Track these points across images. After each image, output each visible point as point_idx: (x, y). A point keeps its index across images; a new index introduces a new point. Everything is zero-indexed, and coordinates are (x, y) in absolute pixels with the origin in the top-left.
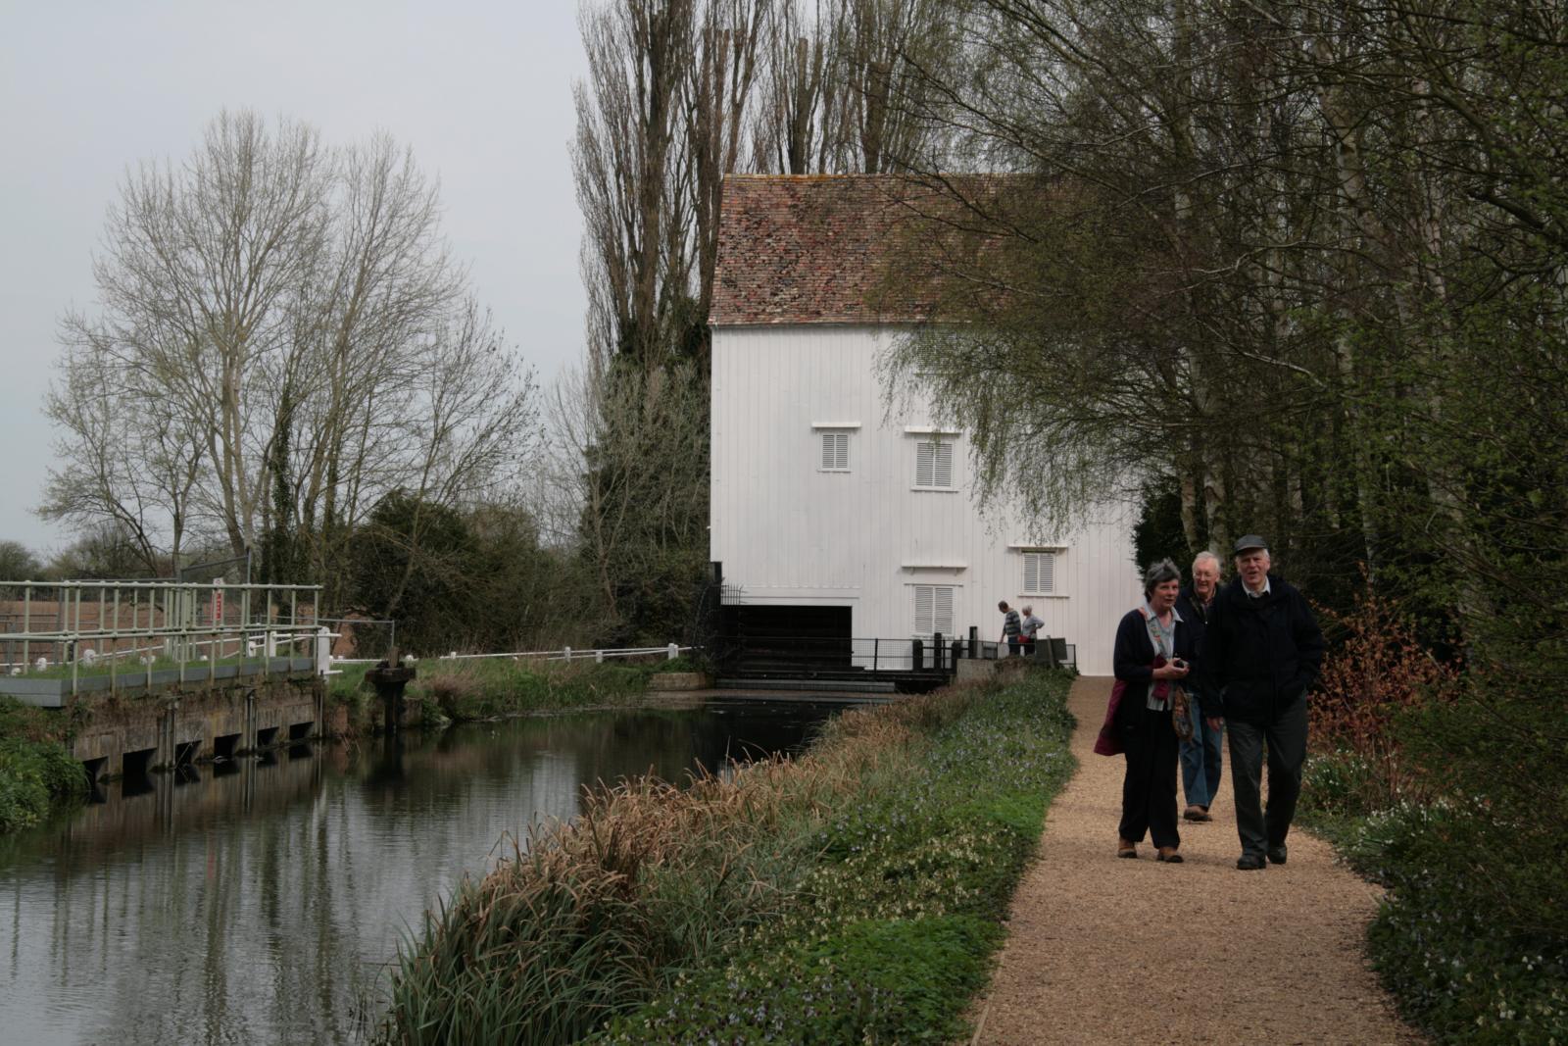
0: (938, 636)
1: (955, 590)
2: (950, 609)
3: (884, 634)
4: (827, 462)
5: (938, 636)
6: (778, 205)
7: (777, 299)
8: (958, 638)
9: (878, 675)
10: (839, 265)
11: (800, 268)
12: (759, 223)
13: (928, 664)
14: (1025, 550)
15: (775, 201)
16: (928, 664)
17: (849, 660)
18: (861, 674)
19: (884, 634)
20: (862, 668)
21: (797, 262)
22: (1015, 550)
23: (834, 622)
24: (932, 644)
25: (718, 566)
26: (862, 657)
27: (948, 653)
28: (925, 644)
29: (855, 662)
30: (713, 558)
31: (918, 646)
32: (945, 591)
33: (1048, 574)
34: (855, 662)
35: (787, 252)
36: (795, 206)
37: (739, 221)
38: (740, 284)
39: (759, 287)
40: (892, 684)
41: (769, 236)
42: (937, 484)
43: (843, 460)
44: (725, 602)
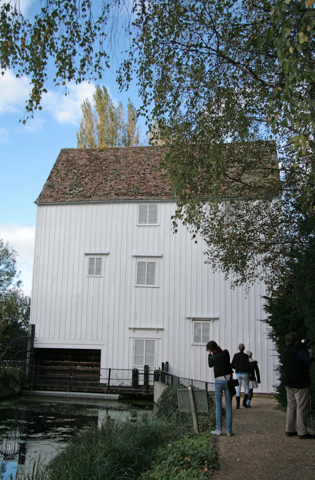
0: (146, 367)
1: (156, 341)
2: (153, 352)
3: (118, 365)
4: (91, 271)
5: (146, 367)
6: (82, 159)
7: (72, 192)
8: (157, 369)
9: (111, 389)
10: (105, 179)
11: (86, 180)
12: (72, 165)
13: (141, 383)
14: (194, 319)
15: (81, 157)
16: (141, 383)
17: (99, 380)
19: (118, 365)
21: (85, 178)
22: (189, 318)
24: (143, 372)
25: (33, 326)
27: (151, 378)
28: (140, 372)
29: (101, 381)
30: (31, 322)
31: (135, 373)
32: (150, 342)
33: (207, 331)
34: (101, 381)
35: (81, 174)
36: (90, 158)
37: (63, 164)
38: (56, 187)
39: (65, 188)
40: (117, 396)
41: (75, 169)
42: (148, 283)
44: (36, 346)
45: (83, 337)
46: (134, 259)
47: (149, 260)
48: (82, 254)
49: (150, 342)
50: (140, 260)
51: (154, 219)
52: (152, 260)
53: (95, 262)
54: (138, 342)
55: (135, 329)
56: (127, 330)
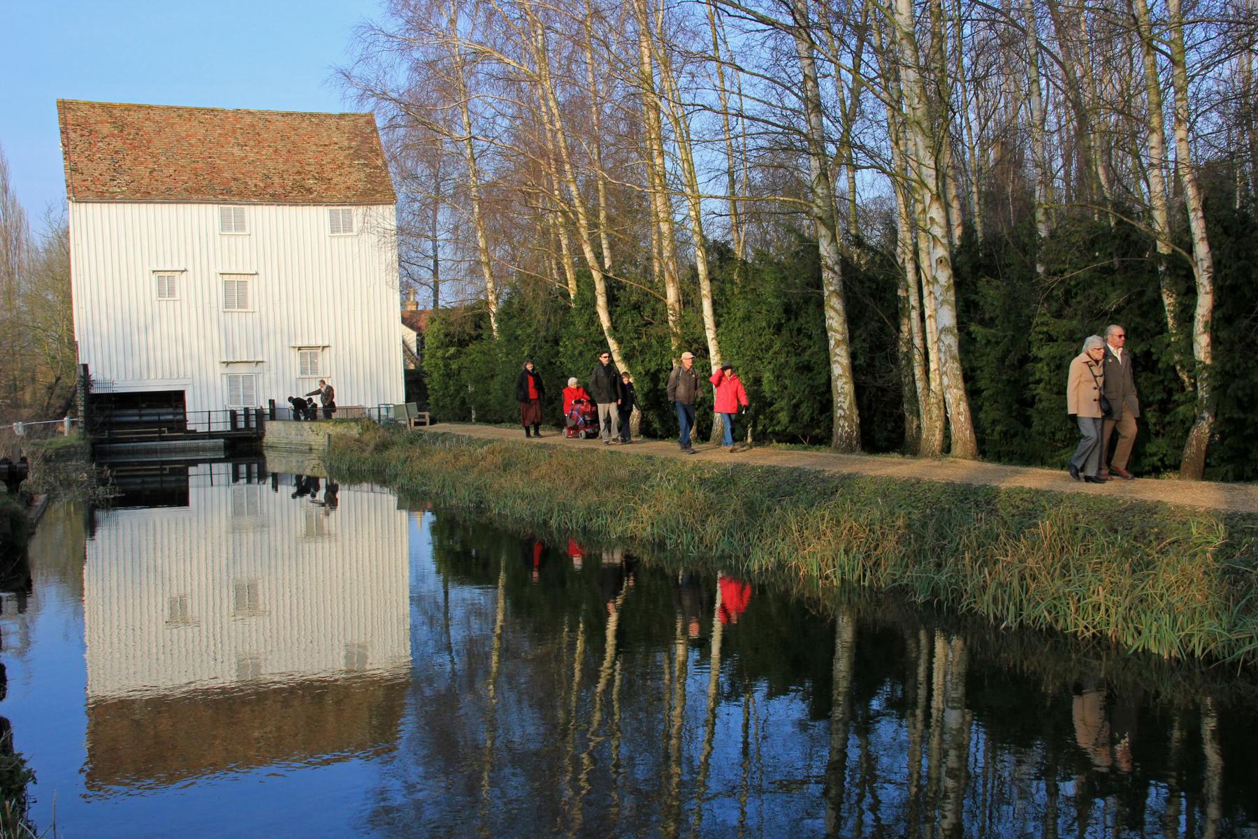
4: (161, 294)
9: (211, 435)
13: (241, 425)
14: (300, 349)
16: (241, 425)
18: (195, 435)
20: (194, 431)
23: (175, 399)
25: (85, 367)
26: (194, 422)
31: (234, 415)
43: (172, 292)
45: (160, 376)
46: (220, 278)
47: (239, 278)
48: (148, 269)
49: (248, 378)
50: (226, 278)
51: (241, 226)
52: (243, 278)
53: (166, 282)
54: (233, 380)
55: (228, 363)
56: (218, 365)
